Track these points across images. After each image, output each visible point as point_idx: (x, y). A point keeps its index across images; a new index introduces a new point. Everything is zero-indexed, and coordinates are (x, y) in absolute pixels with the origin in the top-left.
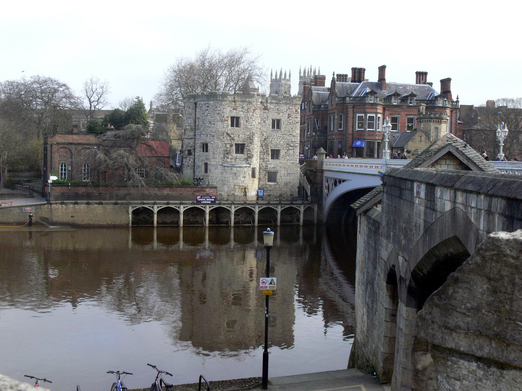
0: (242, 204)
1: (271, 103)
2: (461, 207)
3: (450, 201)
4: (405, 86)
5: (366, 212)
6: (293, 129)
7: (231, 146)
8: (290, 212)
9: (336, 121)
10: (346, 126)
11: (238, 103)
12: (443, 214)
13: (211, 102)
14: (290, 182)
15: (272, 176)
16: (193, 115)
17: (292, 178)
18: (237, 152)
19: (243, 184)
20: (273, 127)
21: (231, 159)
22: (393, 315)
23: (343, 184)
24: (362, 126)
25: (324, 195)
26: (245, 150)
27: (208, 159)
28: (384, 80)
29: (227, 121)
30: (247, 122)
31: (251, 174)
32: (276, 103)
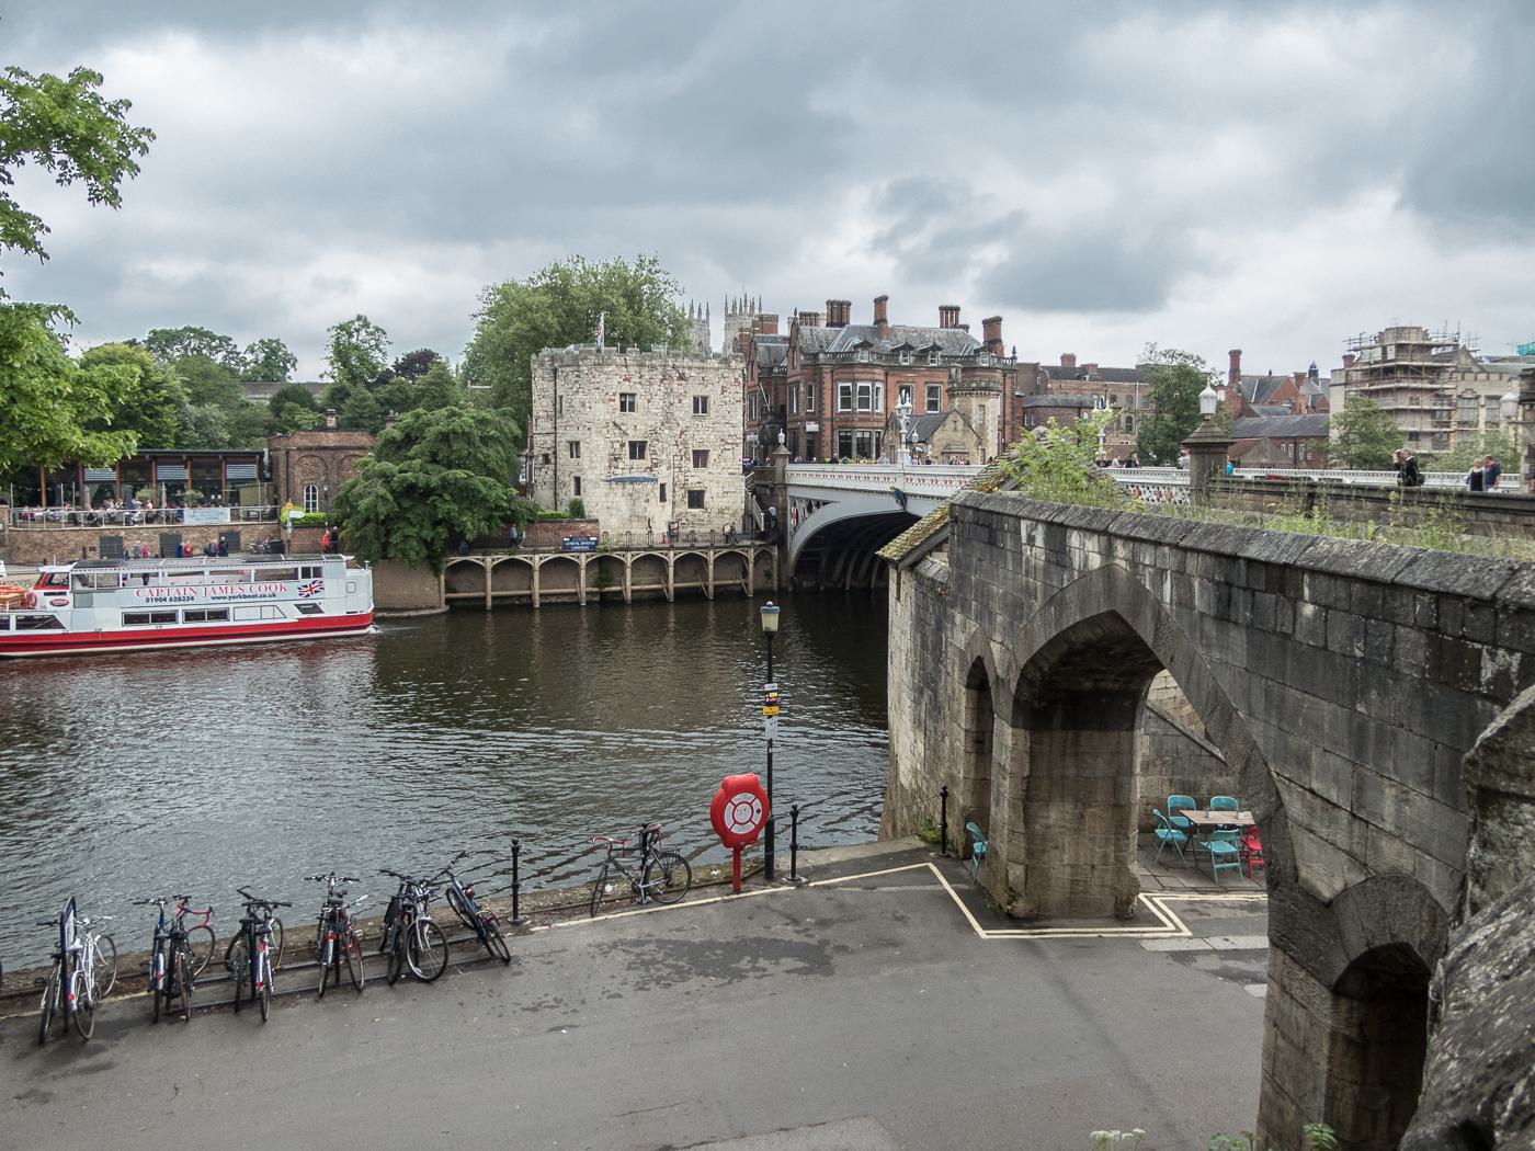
0: (645, 549)
2: (1123, 564)
3: (1099, 553)
4: (920, 332)
5: (912, 567)
7: (623, 445)
8: (731, 558)
9: (802, 395)
10: (821, 404)
11: (632, 370)
12: (1085, 573)
15: (696, 499)
16: (552, 391)
17: (731, 500)
19: (647, 514)
20: (696, 410)
22: (981, 743)
23: (823, 509)
24: (846, 403)
25: (790, 529)
26: (647, 453)
28: (885, 321)
30: (649, 401)
31: (658, 494)
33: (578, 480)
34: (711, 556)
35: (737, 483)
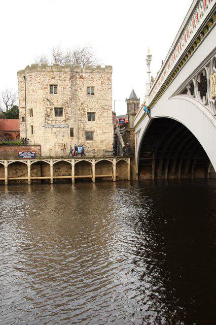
1: (86, 72)
6: (107, 94)
7: (51, 110)
8: (103, 164)
11: (55, 73)
13: (33, 73)
14: (106, 140)
15: (89, 136)
17: (107, 136)
18: (56, 115)
21: (52, 121)
27: (32, 122)
29: (47, 88)
32: (90, 73)
33: (32, 127)
34: (93, 163)
35: (110, 128)
